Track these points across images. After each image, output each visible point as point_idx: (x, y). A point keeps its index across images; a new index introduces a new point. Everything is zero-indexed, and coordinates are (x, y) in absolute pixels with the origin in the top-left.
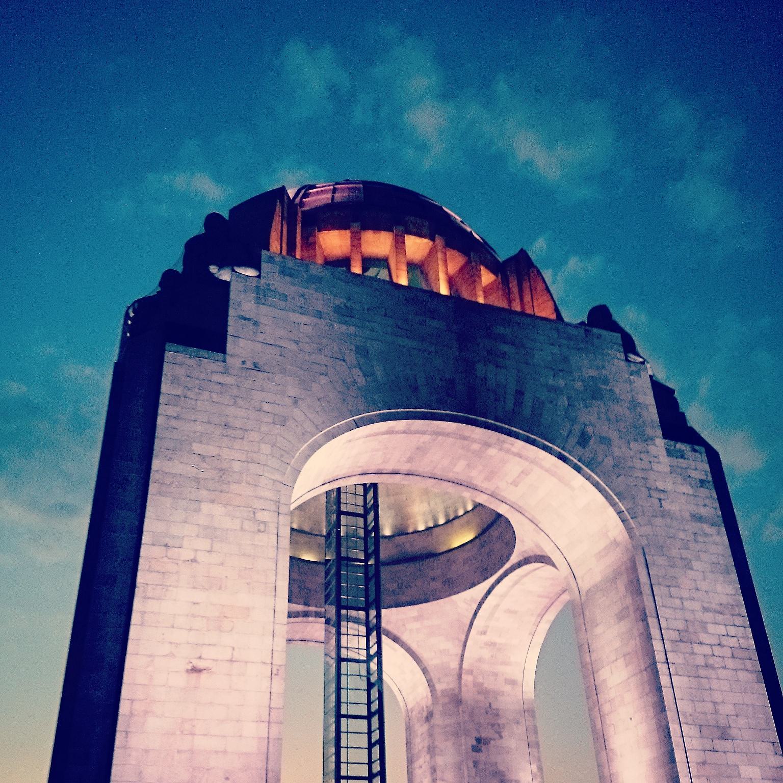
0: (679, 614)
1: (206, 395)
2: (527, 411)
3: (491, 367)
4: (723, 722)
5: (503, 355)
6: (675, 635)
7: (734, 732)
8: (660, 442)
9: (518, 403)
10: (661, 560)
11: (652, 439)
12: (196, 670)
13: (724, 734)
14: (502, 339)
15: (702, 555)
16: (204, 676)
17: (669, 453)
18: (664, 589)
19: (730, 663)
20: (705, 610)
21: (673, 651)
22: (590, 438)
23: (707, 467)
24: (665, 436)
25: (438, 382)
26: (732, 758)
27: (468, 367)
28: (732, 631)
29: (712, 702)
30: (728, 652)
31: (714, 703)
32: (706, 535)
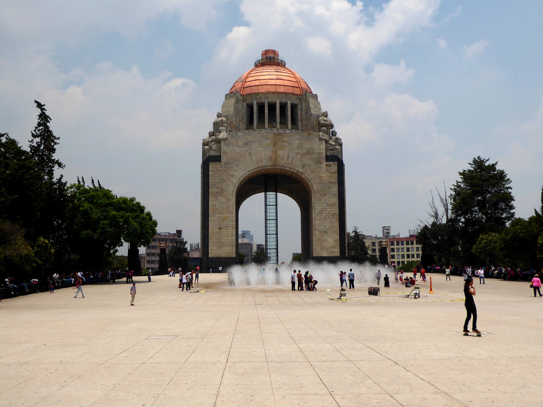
0: (320, 207)
1: (218, 173)
2: (289, 161)
3: (281, 151)
4: (326, 230)
5: (285, 146)
6: (318, 212)
7: (328, 232)
8: (325, 163)
9: (288, 160)
10: (318, 195)
11: (322, 163)
12: (220, 229)
13: (326, 232)
14: (285, 141)
15: (329, 192)
16: (221, 230)
17: (327, 165)
18: (318, 202)
19: (331, 217)
20: (327, 205)
21: (317, 216)
22: (305, 165)
23: (337, 168)
24: (326, 161)
25: (268, 158)
26: (326, 237)
27: (276, 152)
28: (333, 210)
29: (324, 226)
30: (331, 215)
31: (324, 226)
32: (332, 187)
